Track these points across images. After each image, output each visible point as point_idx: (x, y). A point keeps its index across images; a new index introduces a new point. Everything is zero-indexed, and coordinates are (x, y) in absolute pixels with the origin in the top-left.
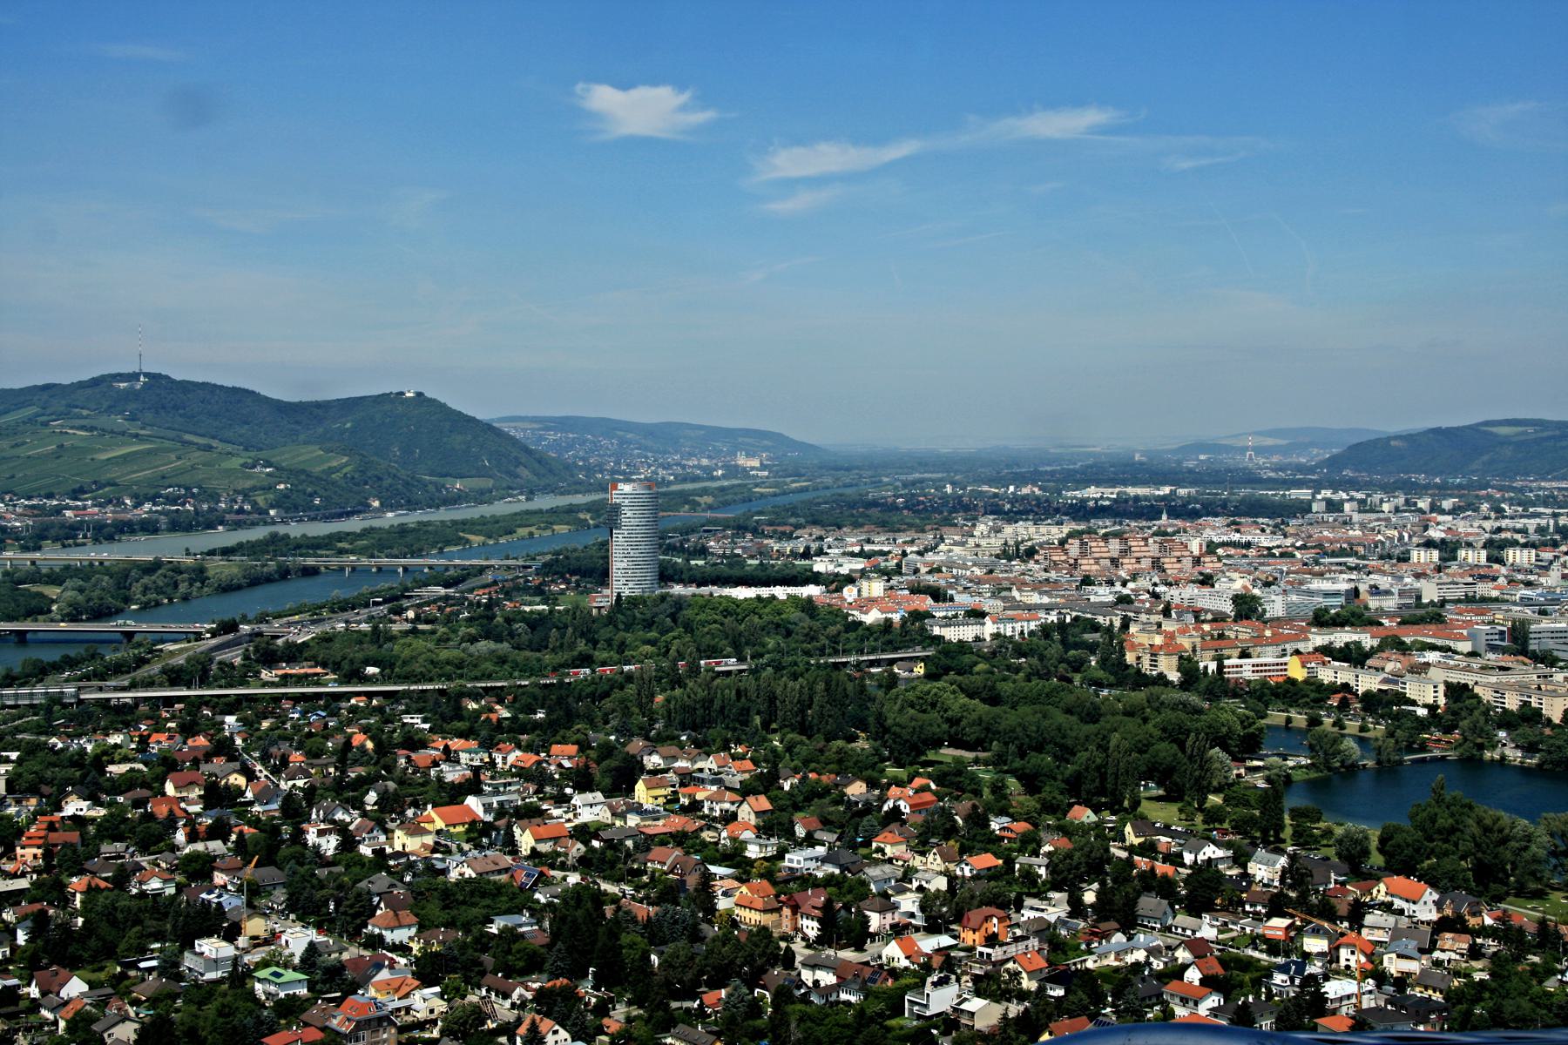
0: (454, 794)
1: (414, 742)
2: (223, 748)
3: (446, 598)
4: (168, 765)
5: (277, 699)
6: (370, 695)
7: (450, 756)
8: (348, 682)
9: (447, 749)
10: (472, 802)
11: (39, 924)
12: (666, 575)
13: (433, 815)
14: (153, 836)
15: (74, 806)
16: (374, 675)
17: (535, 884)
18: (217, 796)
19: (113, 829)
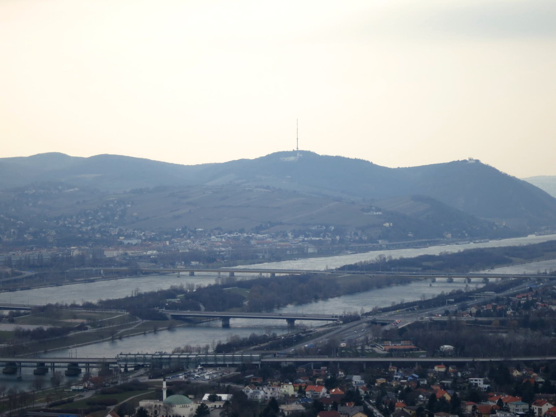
3: (497, 300)
5: (386, 365)
6: (447, 364)
8: (433, 356)
9: (500, 402)
16: (449, 350)
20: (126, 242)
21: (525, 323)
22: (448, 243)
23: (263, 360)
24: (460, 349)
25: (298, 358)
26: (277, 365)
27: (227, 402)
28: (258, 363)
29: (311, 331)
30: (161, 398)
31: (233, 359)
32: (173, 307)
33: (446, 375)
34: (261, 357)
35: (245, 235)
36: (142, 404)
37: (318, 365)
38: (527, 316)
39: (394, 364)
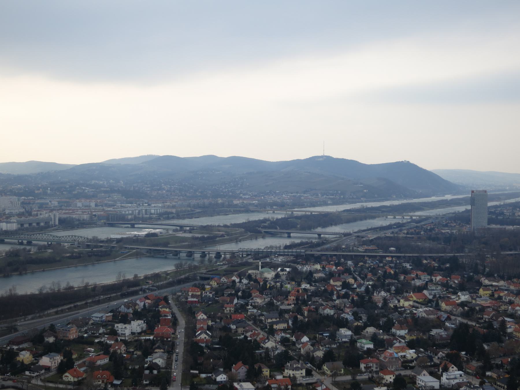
0: (419, 290)
1: (406, 272)
2: (348, 271)
3: (417, 227)
4: (331, 275)
5: (363, 256)
6: (392, 257)
7: (418, 277)
8: (386, 253)
9: (417, 275)
10: (425, 292)
11: (295, 320)
12: (490, 221)
13: (413, 296)
14: (327, 295)
15: (304, 286)
16: (393, 250)
17: (446, 320)
18: (346, 285)
19: (316, 294)
20: (243, 197)
21: (430, 238)
22: (394, 200)
23: (306, 253)
24: (399, 250)
25: (322, 252)
26: (312, 255)
27: (289, 272)
28: (303, 254)
29: (329, 240)
30: (258, 270)
31: (292, 252)
32: (265, 227)
33: (391, 262)
34: (305, 252)
35: (299, 195)
36: (250, 272)
37: (331, 256)
38: (431, 235)
39: (368, 256)
